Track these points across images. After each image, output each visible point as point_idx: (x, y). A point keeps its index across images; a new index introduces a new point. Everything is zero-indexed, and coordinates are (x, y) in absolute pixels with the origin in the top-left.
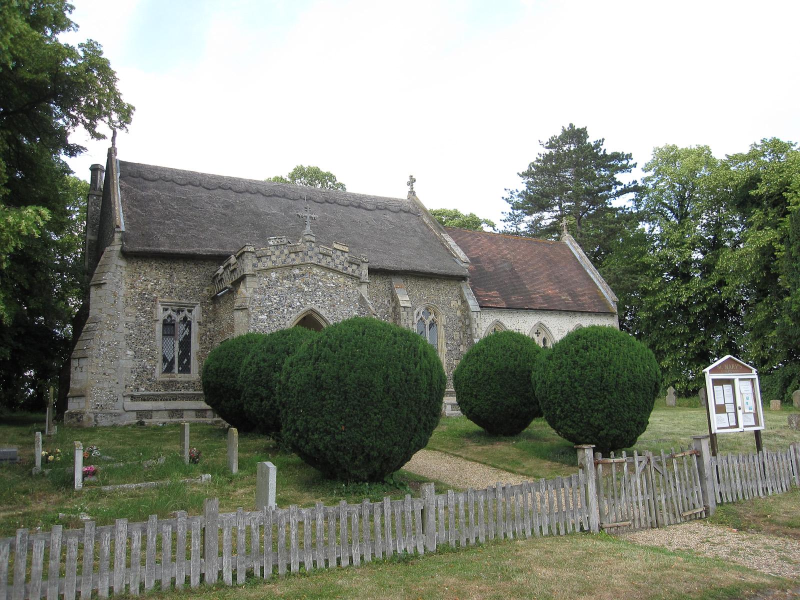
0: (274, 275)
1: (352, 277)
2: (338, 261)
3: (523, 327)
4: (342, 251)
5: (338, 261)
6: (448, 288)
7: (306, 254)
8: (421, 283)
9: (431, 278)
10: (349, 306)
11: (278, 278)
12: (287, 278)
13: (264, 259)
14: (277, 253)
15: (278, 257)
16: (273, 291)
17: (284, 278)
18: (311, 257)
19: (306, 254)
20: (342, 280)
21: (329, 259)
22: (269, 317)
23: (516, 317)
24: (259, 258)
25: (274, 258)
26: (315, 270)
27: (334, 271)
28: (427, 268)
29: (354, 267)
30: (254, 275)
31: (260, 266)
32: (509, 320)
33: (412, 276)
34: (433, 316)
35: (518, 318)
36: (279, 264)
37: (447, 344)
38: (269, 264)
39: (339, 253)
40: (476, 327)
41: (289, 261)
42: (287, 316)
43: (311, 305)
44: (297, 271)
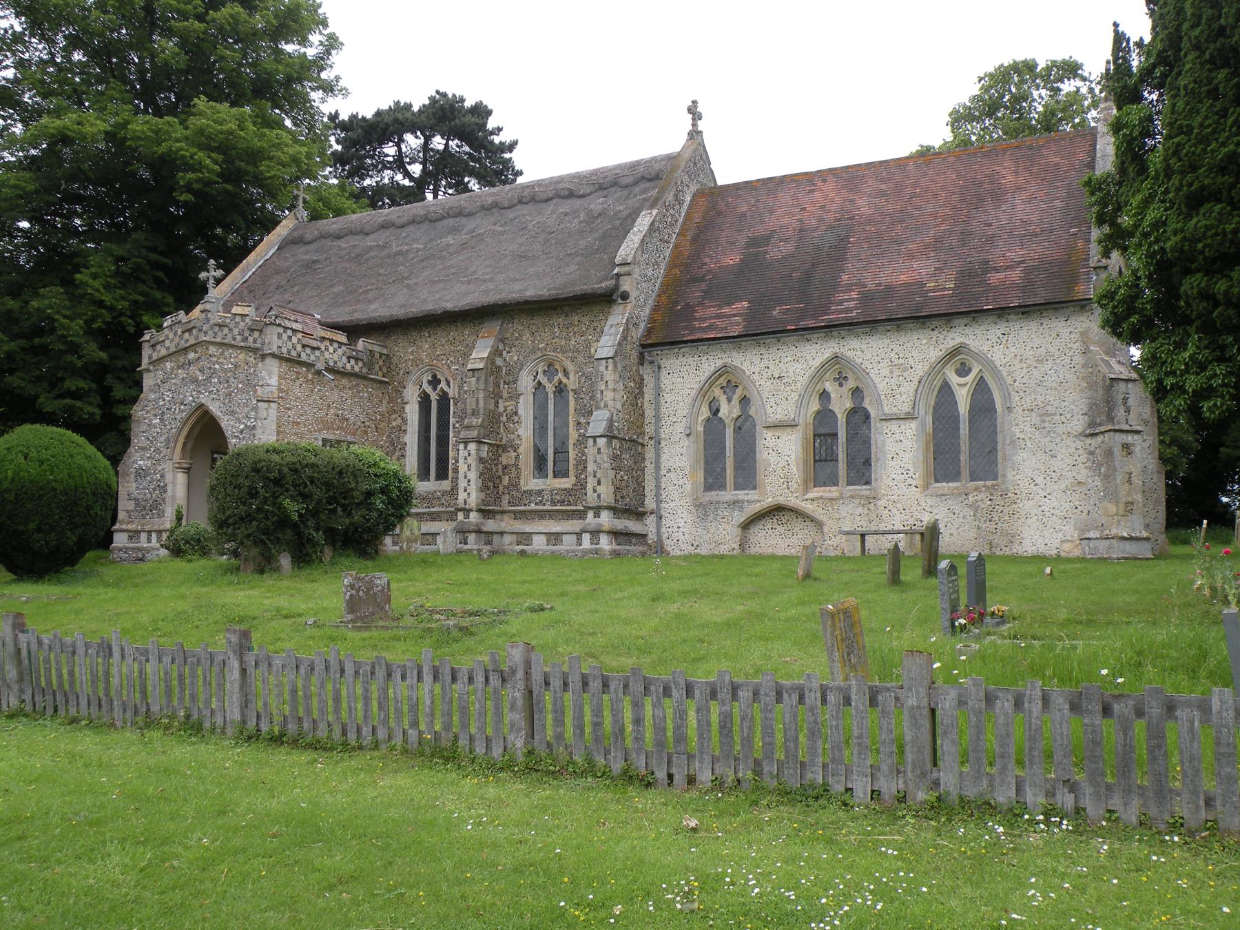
0: (169, 365)
1: (255, 350)
2: (236, 331)
3: (791, 370)
4: (242, 315)
5: (236, 331)
6: (586, 320)
7: (201, 330)
8: (537, 321)
9: (555, 308)
10: (248, 392)
11: (172, 369)
12: (182, 367)
13: (158, 347)
14: (171, 336)
15: (172, 341)
16: (167, 386)
17: (179, 367)
18: (206, 333)
19: (201, 330)
20: (242, 356)
21: (226, 331)
22: (162, 420)
23: (773, 350)
24: (153, 346)
25: (167, 343)
26: (212, 349)
27: (232, 346)
28: (532, 290)
29: (256, 334)
30: (148, 370)
31: (155, 356)
32: (756, 359)
33: (521, 311)
34: (560, 375)
35: (780, 353)
36: (173, 349)
37: (579, 423)
38: (163, 352)
39: (238, 319)
40: (603, 388)
41: (183, 344)
42: (179, 417)
43: (204, 399)
44: (192, 355)
